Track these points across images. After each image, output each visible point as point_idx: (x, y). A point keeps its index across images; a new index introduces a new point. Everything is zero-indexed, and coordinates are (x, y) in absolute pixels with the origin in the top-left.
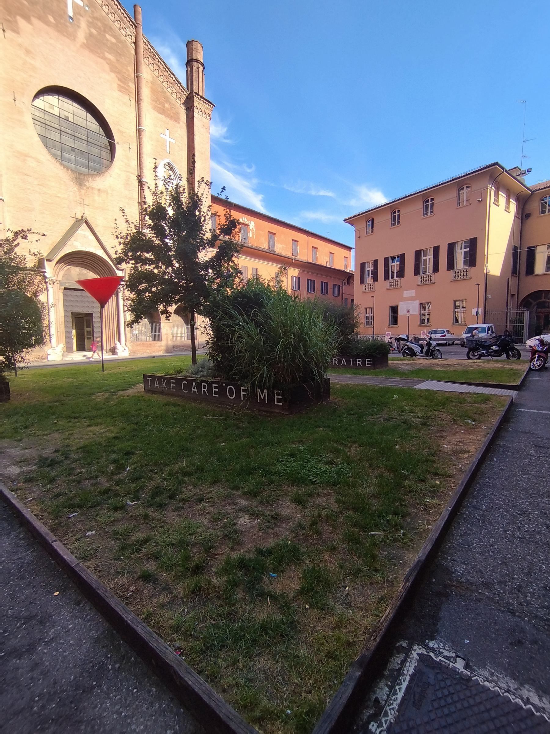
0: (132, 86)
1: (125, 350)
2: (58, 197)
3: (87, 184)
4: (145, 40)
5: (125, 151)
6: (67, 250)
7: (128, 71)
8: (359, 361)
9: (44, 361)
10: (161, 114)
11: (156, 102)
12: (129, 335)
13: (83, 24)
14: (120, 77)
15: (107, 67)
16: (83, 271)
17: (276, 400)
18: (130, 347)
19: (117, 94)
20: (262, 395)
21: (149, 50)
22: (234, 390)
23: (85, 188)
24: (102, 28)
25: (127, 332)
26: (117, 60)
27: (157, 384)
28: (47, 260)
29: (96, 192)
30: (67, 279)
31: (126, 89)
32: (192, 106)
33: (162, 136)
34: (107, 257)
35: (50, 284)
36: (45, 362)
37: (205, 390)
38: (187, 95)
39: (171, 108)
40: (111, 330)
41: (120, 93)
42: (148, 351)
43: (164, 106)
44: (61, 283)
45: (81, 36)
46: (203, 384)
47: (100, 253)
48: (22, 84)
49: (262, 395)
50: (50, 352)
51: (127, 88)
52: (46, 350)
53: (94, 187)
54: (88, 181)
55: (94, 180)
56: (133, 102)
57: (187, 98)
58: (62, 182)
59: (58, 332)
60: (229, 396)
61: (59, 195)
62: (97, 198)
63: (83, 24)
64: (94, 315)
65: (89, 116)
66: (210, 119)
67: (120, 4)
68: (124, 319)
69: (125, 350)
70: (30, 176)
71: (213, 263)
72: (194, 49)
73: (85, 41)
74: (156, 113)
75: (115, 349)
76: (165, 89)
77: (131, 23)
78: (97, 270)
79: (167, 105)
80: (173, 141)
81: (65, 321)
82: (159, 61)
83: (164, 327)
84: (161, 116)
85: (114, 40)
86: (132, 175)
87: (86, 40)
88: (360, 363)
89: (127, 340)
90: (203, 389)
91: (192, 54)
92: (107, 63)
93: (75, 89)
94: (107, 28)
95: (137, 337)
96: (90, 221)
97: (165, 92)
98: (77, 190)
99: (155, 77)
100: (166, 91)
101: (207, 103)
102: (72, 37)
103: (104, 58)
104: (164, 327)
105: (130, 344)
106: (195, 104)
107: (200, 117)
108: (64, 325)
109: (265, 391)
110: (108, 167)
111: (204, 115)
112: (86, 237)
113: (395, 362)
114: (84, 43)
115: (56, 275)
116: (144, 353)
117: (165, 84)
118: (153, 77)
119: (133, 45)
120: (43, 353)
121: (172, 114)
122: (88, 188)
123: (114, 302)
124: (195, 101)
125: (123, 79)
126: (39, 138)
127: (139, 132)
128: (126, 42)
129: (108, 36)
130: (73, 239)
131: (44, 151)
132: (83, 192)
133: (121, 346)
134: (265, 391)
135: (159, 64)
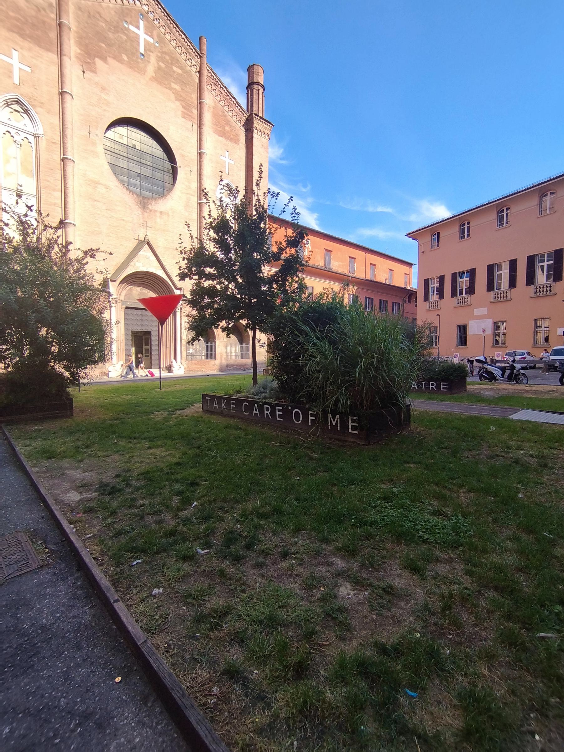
0: (195, 112)
1: (180, 368)
2: (123, 220)
3: (150, 207)
4: (208, 69)
5: (186, 174)
7: (192, 98)
8: (433, 385)
9: (105, 377)
10: (221, 137)
11: (217, 125)
12: (184, 353)
13: (153, 59)
14: (184, 105)
15: (173, 97)
16: (144, 291)
17: (350, 427)
18: (185, 365)
19: (181, 120)
20: (334, 421)
21: (212, 77)
22: (301, 414)
23: (148, 211)
24: (170, 61)
25: (183, 350)
26: (182, 89)
27: (216, 404)
28: (111, 281)
29: (158, 214)
31: (190, 116)
32: (252, 127)
33: (222, 158)
34: (166, 276)
35: (113, 303)
36: (105, 379)
37: (268, 412)
38: (247, 117)
39: (231, 130)
40: (168, 349)
41: (183, 120)
42: (203, 369)
43: (224, 129)
44: (123, 302)
45: (150, 70)
46: (265, 406)
47: (160, 273)
48: (96, 118)
49: (334, 421)
50: (110, 368)
51: (190, 114)
52: (107, 367)
53: (156, 209)
54: (151, 204)
55: (156, 203)
56: (196, 127)
57: (247, 119)
58: (128, 206)
60: (295, 421)
61: (124, 219)
62: (158, 220)
63: (153, 59)
64: (152, 333)
65: (155, 144)
66: (269, 138)
67: (186, 37)
68: (181, 338)
69: (180, 368)
70: (99, 202)
71: (277, 278)
72: (255, 73)
73: (154, 75)
74: (217, 136)
75: (171, 367)
76: (226, 113)
77: (196, 54)
79: (227, 128)
80: (232, 162)
81: (126, 339)
82: (221, 87)
83: (219, 345)
84: (221, 138)
85: (180, 71)
86: (192, 197)
87: (155, 73)
88: (434, 387)
89: (183, 359)
90: (266, 412)
91: (253, 77)
92: (173, 93)
93: (143, 119)
94: (174, 61)
95: (192, 356)
96: (152, 243)
97: (225, 116)
98: (140, 213)
99: (217, 102)
100: (227, 114)
101: (266, 123)
102: (142, 72)
103: (171, 89)
104: (219, 345)
105: (186, 363)
106: (255, 125)
107: (259, 137)
108: (124, 343)
109: (338, 416)
110: (170, 190)
111: (263, 136)
112: (147, 258)
113: (473, 387)
114: (153, 76)
115: (119, 295)
116: (198, 371)
117: (226, 108)
118: (215, 102)
119: (198, 74)
121: (232, 136)
122: (151, 211)
123: (171, 321)
124: (254, 122)
125: (186, 107)
126: (109, 166)
127: (200, 155)
128: (190, 71)
129: (175, 68)
130: (135, 259)
131: (113, 178)
132: (146, 214)
133: (177, 364)
134: (338, 416)
135: (221, 90)
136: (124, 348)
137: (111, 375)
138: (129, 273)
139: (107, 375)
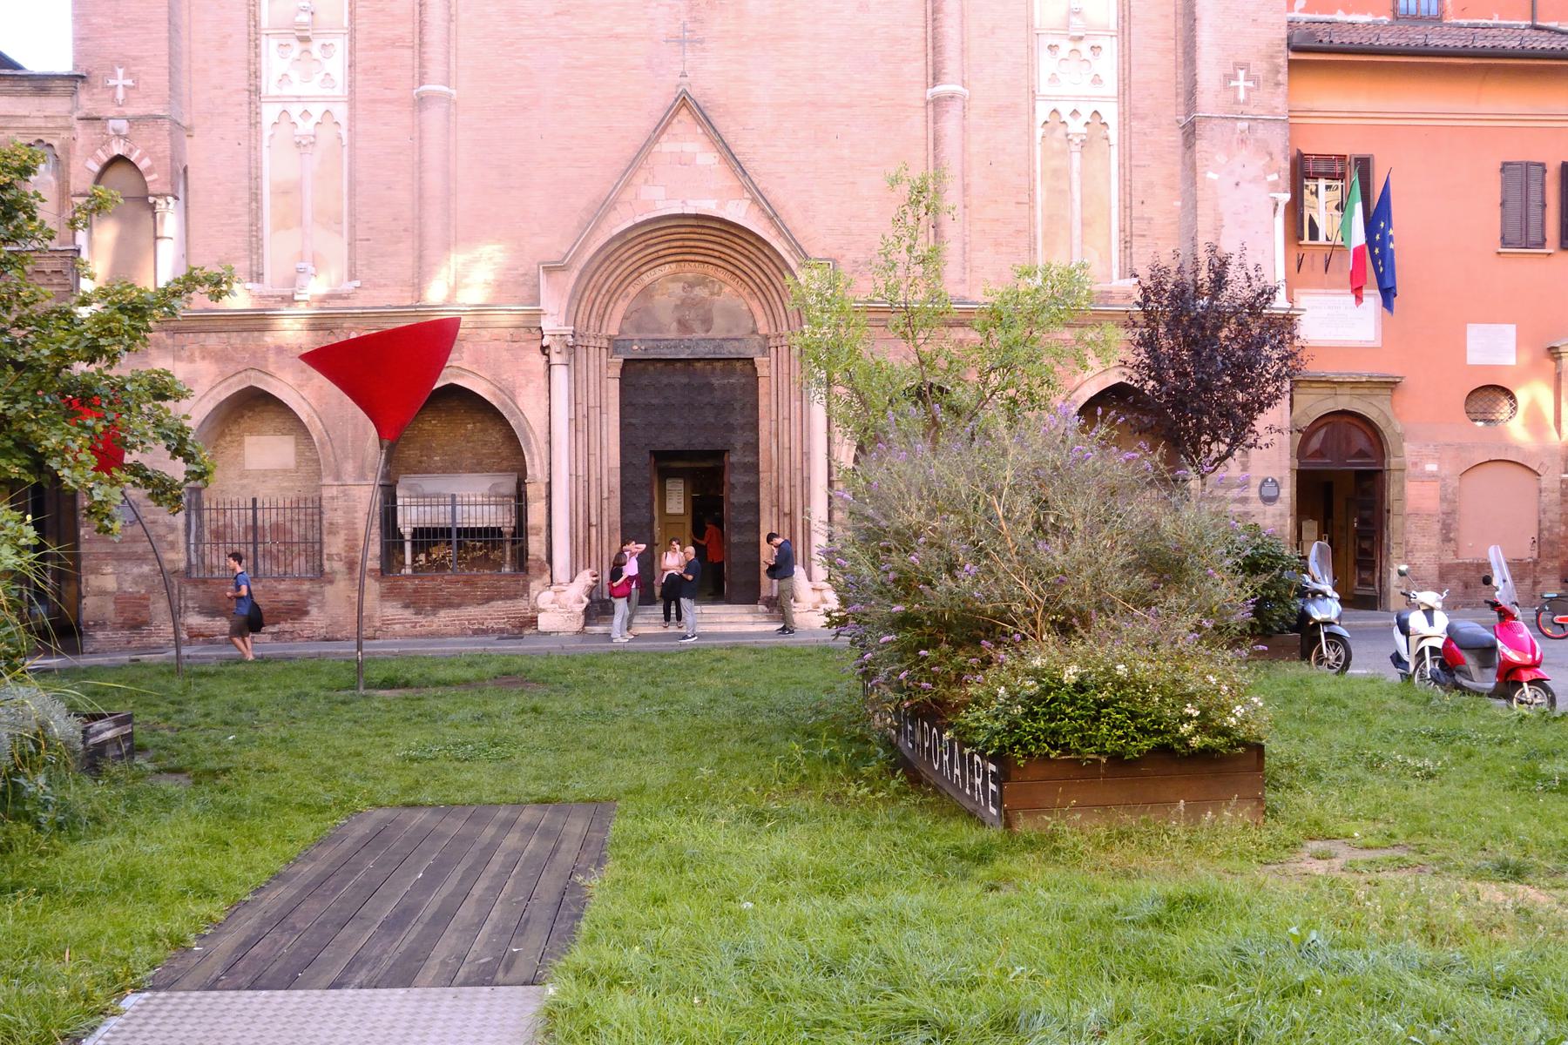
2: (617, 37)
6: (620, 222)
30: (639, 328)
34: (764, 222)
44: (615, 344)
47: (738, 212)
52: (533, 594)
59: (590, 525)
61: (621, 29)
68: (830, 474)
78: (746, 279)
112: (683, 161)
120: (525, 603)
136: (617, 517)
137: (544, 622)
138: (616, 231)
139: (533, 621)
